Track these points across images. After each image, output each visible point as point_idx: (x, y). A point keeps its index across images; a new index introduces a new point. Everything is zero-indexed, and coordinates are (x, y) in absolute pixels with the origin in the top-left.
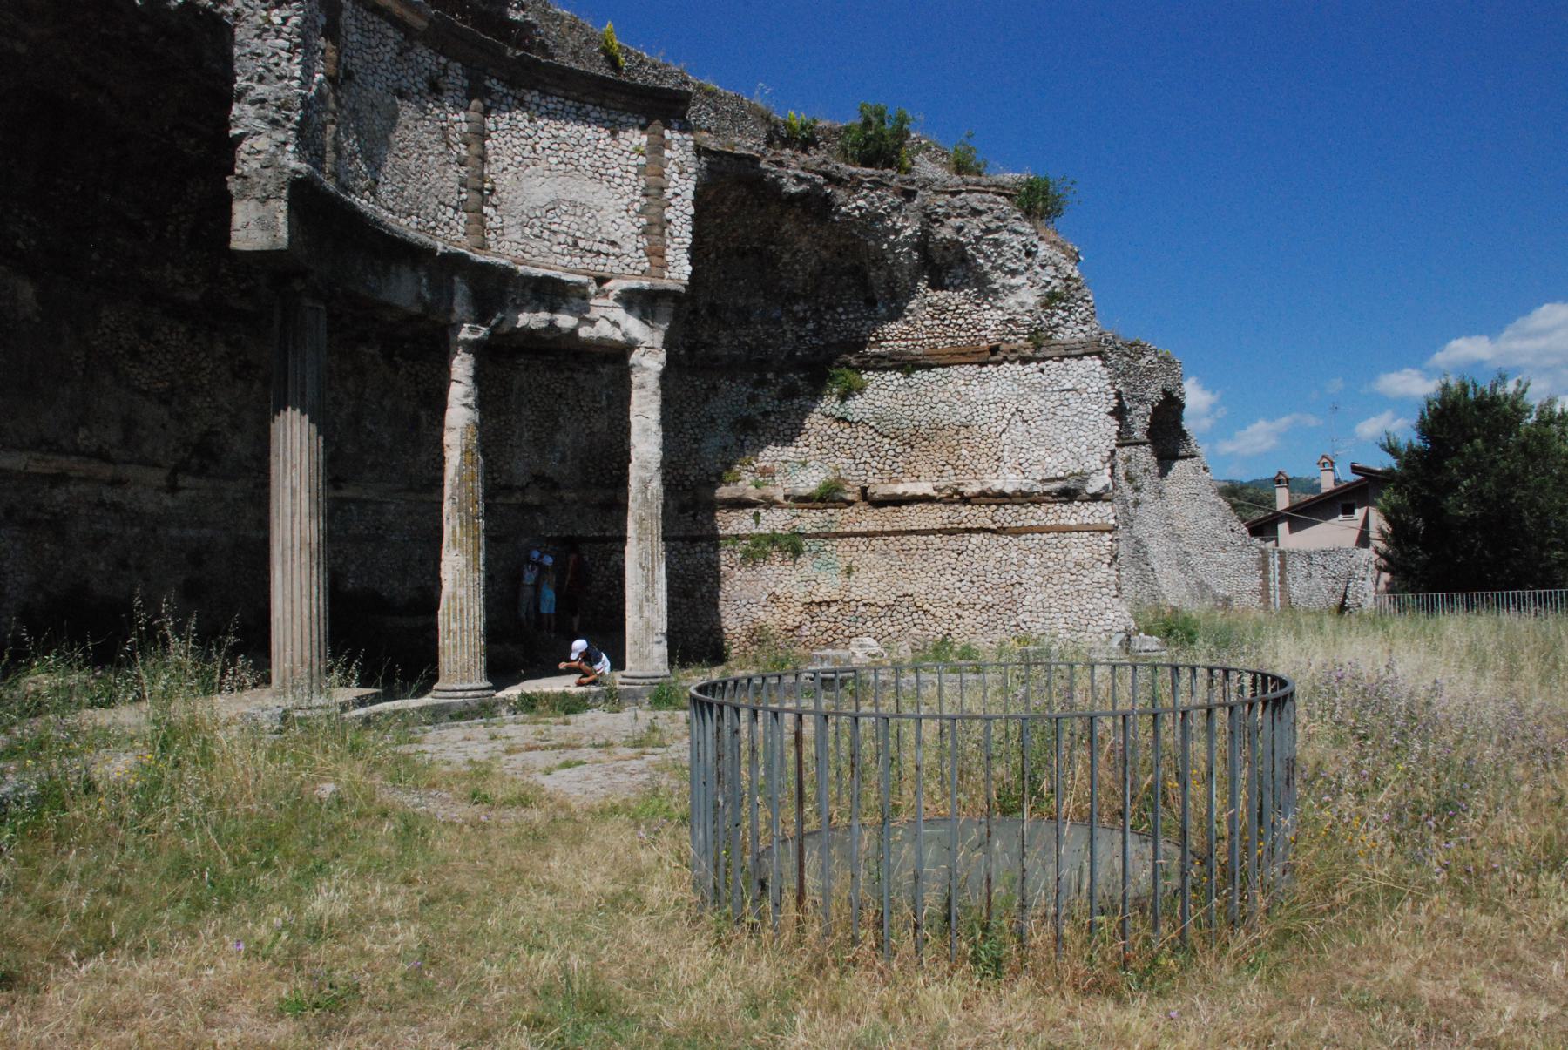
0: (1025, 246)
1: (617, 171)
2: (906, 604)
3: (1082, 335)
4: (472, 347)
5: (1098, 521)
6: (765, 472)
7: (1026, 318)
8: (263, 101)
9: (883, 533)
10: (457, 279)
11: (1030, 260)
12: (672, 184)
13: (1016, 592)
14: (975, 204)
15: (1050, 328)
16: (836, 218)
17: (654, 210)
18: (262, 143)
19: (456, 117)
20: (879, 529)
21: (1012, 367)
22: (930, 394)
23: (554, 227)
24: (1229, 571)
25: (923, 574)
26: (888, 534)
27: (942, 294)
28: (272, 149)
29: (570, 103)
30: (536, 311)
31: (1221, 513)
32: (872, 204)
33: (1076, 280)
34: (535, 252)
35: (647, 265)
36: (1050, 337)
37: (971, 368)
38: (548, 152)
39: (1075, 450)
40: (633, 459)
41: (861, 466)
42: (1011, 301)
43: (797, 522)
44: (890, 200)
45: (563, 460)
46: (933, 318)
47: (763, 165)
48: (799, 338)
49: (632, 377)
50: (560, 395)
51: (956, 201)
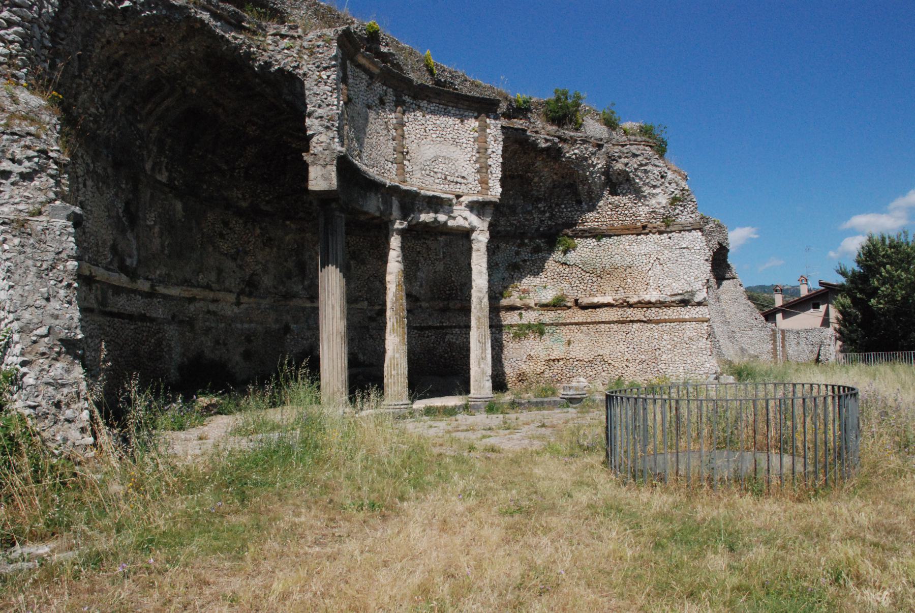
0: (660, 173)
1: (464, 140)
2: (599, 360)
3: (691, 220)
4: (402, 232)
5: (701, 316)
6: (524, 291)
7: (661, 211)
8: (321, 117)
9: (586, 323)
10: (393, 198)
11: (663, 180)
12: (491, 146)
13: (657, 353)
14: (635, 151)
15: (674, 216)
16: (564, 159)
17: (482, 160)
18: (323, 138)
19: (391, 116)
20: (585, 321)
21: (654, 236)
22: (611, 250)
23: (436, 170)
24: (754, 341)
25: (608, 345)
26: (590, 323)
27: (617, 198)
28: (328, 141)
29: (441, 106)
30: (428, 213)
31: (749, 310)
32: (582, 152)
33: (687, 191)
34: (427, 183)
35: (480, 188)
36: (674, 221)
37: (632, 237)
38: (432, 132)
39: (688, 279)
40: (474, 287)
41: (575, 288)
42: (653, 202)
43: (541, 317)
44: (590, 149)
45: (421, 286)
46: (611, 210)
47: (528, 133)
48: (542, 221)
49: (473, 245)
50: (419, 252)
51: (624, 150)
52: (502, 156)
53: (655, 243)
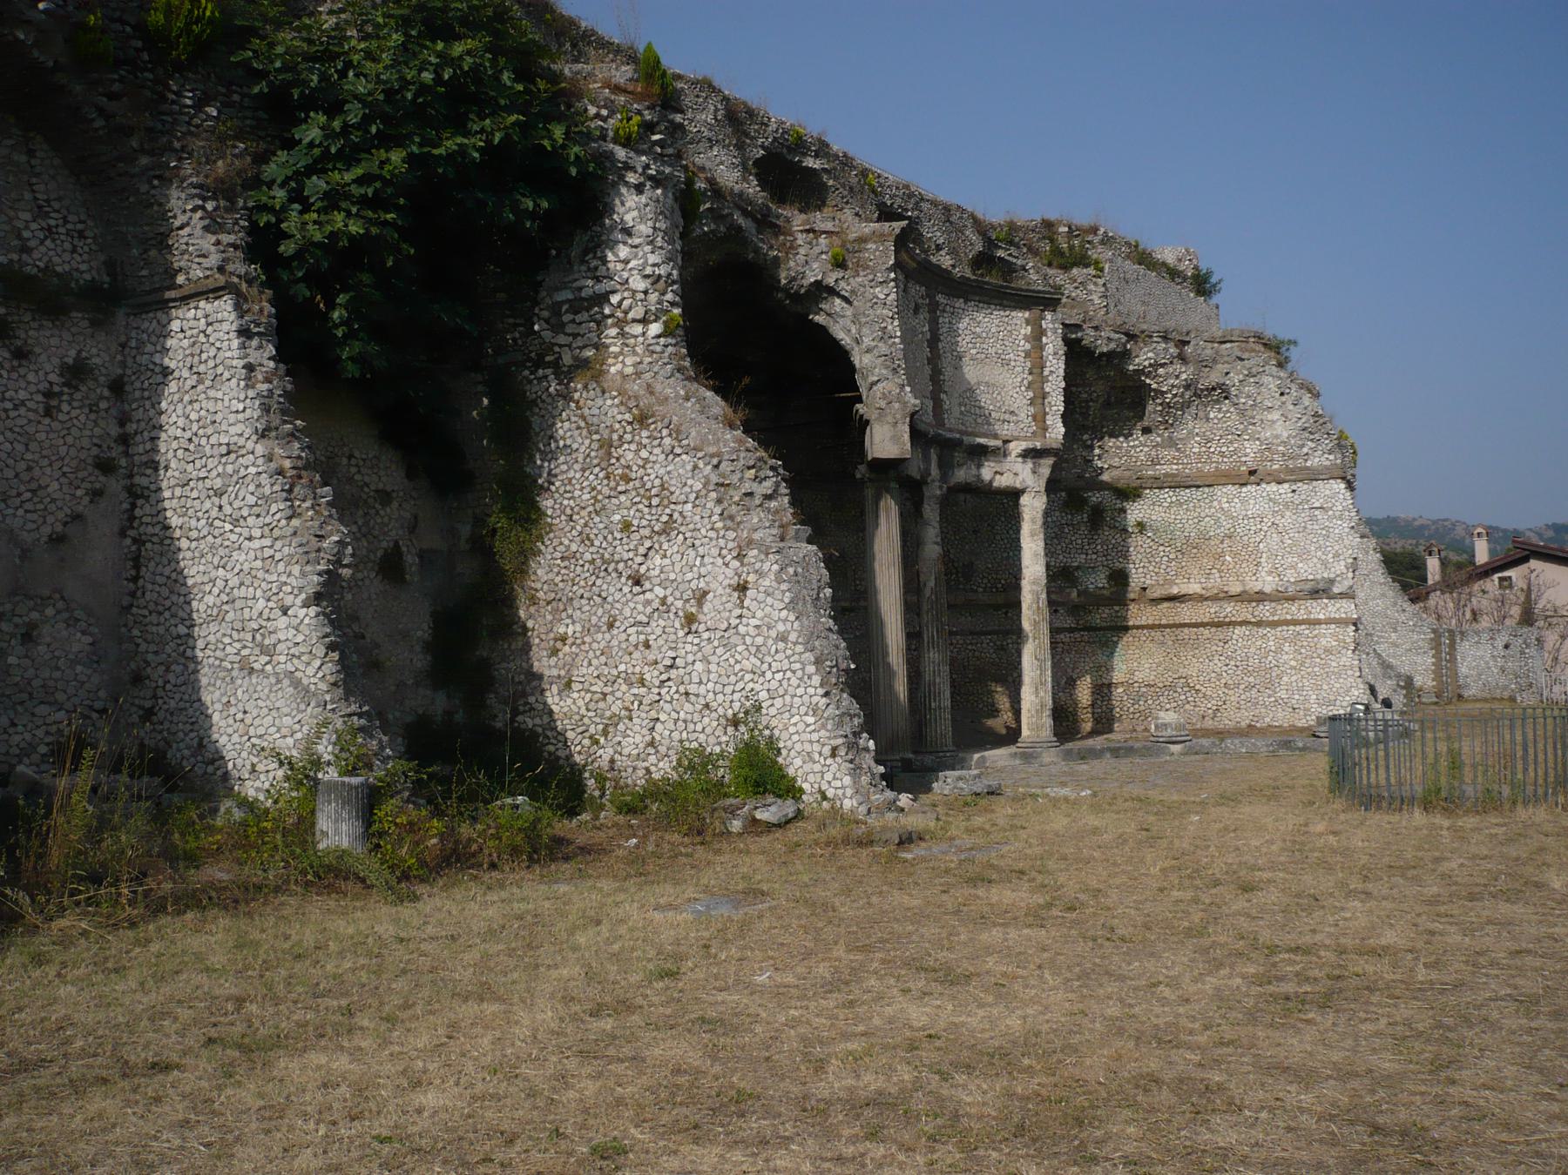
9: (1160, 626)
12: (1048, 364)
13: (1274, 674)
20: (1157, 622)
25: (1195, 660)
26: (1166, 626)
41: (1141, 570)
52: (1065, 378)
53: (1270, 500)
